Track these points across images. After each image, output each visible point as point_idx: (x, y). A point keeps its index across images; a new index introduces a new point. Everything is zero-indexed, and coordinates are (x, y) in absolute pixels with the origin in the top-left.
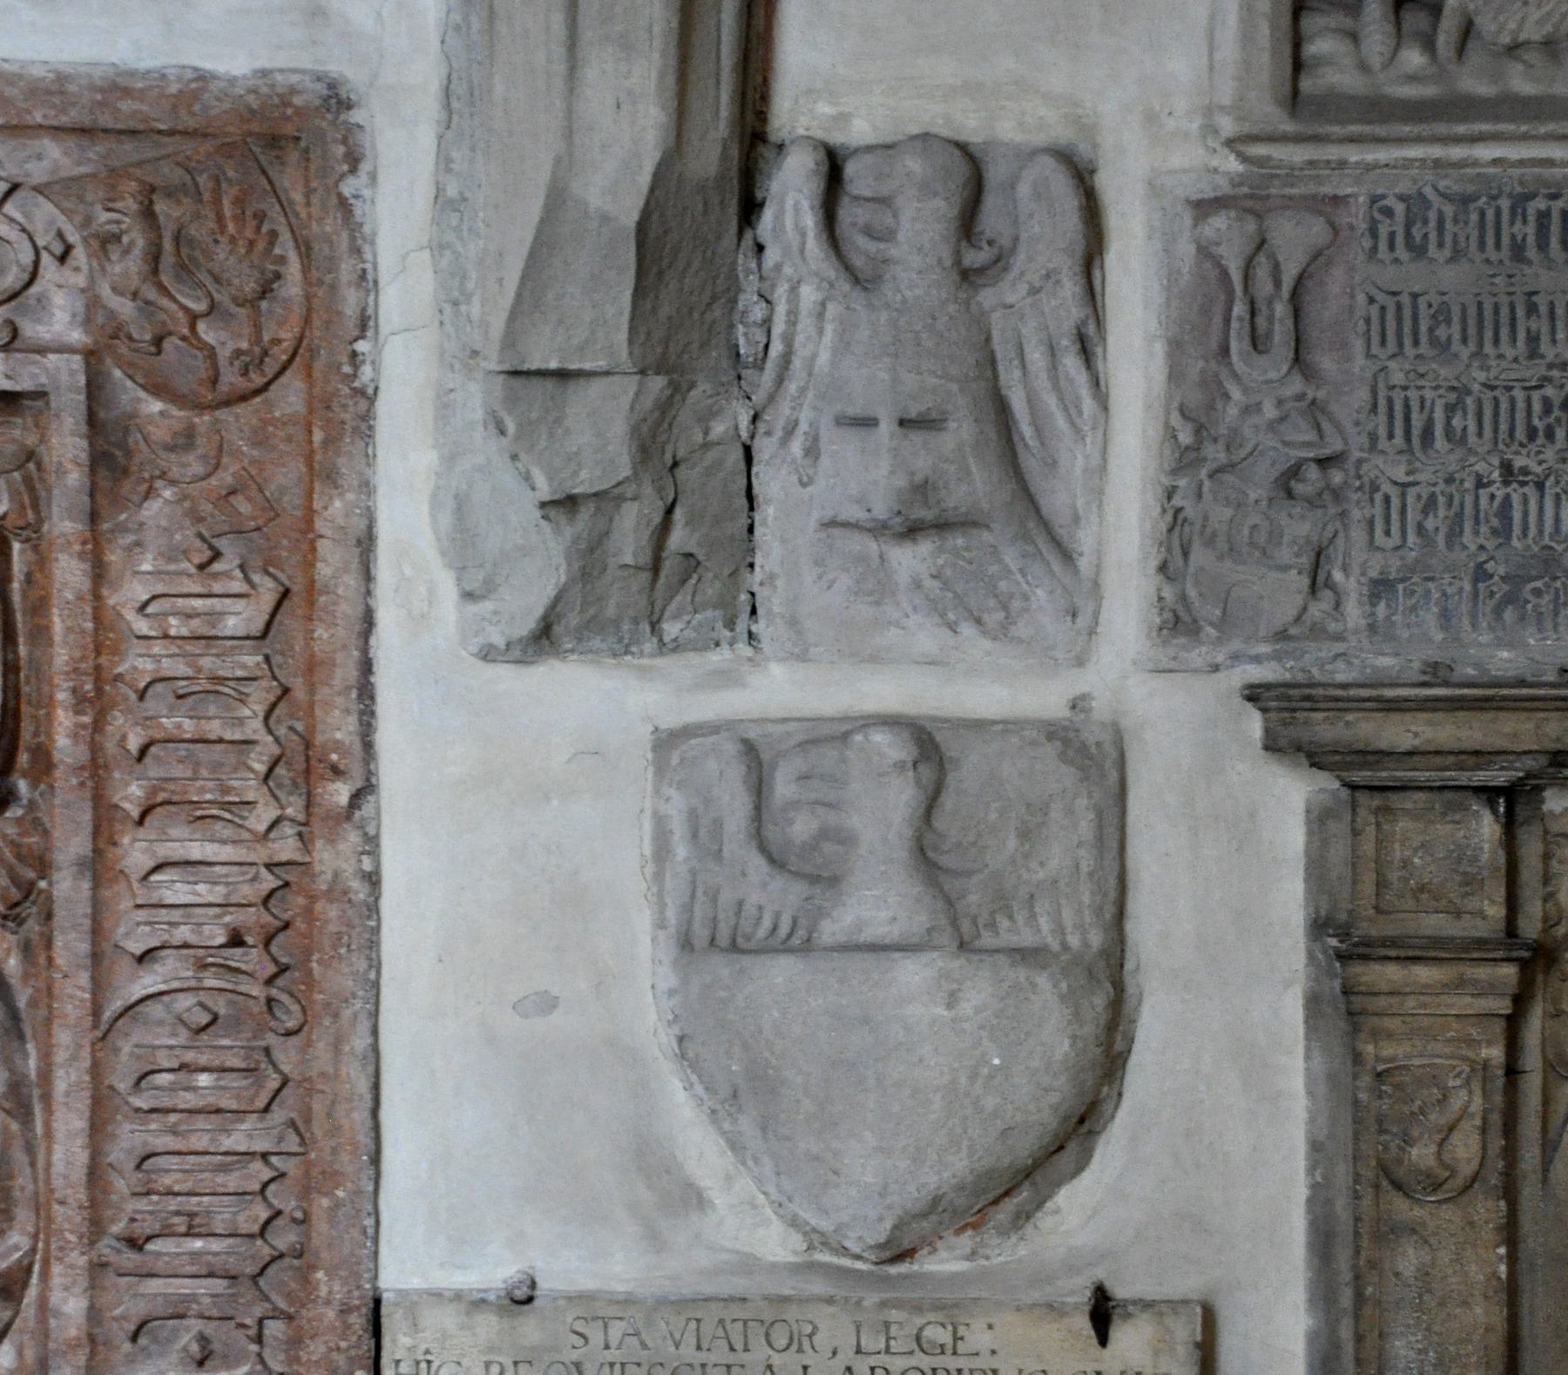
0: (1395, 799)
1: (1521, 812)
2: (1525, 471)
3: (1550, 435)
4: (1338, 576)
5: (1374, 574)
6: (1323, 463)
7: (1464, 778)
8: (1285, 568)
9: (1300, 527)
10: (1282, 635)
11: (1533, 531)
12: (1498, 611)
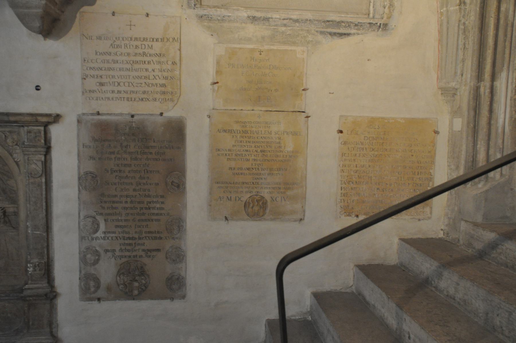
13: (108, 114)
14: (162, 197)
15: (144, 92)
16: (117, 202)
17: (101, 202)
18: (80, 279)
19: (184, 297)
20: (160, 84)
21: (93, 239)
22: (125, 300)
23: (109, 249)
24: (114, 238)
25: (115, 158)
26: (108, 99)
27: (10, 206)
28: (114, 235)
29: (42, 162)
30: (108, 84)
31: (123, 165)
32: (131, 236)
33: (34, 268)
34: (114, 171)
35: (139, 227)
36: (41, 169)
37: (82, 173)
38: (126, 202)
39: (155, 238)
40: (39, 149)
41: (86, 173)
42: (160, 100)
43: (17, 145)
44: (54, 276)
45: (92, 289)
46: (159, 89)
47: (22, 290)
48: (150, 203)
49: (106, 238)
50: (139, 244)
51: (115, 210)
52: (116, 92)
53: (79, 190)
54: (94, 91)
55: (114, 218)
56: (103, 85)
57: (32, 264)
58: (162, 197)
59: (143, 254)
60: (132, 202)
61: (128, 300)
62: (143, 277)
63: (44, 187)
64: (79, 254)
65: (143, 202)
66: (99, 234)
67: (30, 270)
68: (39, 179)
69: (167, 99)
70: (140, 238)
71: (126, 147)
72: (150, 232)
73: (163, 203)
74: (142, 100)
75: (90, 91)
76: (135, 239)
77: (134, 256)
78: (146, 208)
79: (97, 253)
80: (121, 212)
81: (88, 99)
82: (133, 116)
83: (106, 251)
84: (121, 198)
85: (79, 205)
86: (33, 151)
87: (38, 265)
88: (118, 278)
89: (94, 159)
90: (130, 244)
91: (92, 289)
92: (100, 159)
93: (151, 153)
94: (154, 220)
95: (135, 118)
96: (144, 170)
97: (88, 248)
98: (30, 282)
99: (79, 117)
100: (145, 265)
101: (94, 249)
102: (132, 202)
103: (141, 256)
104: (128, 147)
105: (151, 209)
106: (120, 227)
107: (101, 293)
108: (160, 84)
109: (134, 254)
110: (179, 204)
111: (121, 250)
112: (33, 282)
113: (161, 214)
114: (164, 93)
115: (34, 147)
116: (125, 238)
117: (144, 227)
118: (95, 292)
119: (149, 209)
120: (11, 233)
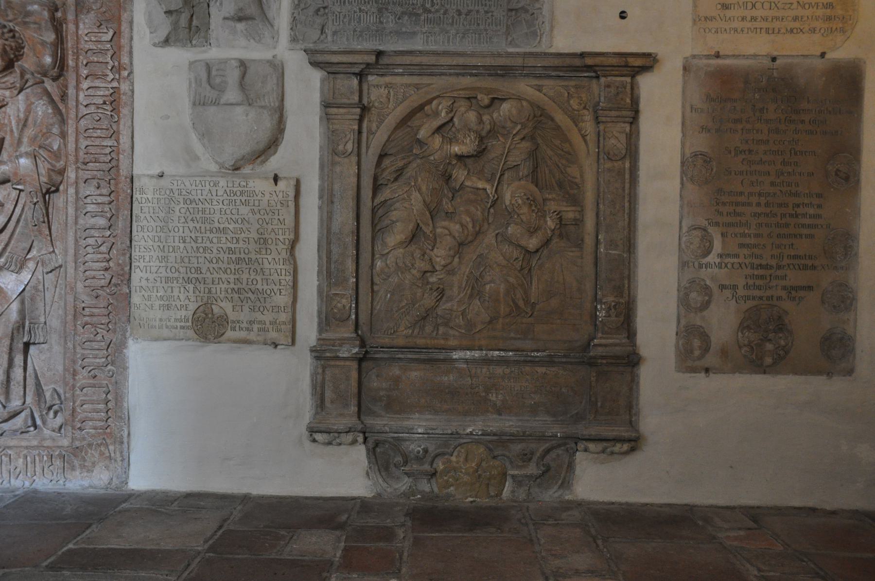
0: (337, 76)
1: (363, 80)
2: (364, 10)
3: (369, 3)
4: (327, 31)
5: (333, 30)
6: (325, 8)
7: (349, 70)
8: (315, 29)
9: (319, 20)
10: (315, 42)
11: (365, 22)
12: (358, 38)
13: (734, 56)
14: (819, 196)
15: (795, 19)
16: (744, 204)
17: (718, 204)
18: (677, 334)
19: (850, 372)
20: (823, 3)
21: (700, 266)
22: (751, 373)
23: (728, 283)
24: (737, 266)
25: (742, 129)
26: (736, 30)
27: (569, 209)
28: (735, 260)
29: (627, 134)
30: (736, 6)
31: (755, 142)
32: (764, 263)
33: (607, 312)
34: (741, 152)
35: (779, 247)
36: (625, 145)
37: (688, 152)
38: (759, 204)
39: (805, 267)
40: (624, 113)
41: (695, 155)
42: (822, 31)
43: (585, 108)
44: (636, 328)
45: (697, 353)
46: (820, 12)
47: (587, 347)
48: (798, 206)
49: (723, 265)
50: (777, 277)
51: (739, 218)
52: (749, 19)
53: (682, 183)
54: (712, 19)
55: (738, 230)
56: (727, 8)
57: (604, 304)
58: (819, 196)
59: (784, 294)
60: (767, 205)
61: (756, 374)
62: (781, 335)
63: (627, 176)
64: (678, 290)
65: (786, 205)
66: (712, 258)
67: (601, 314)
68: (620, 162)
69: (834, 29)
70: (779, 267)
71: (761, 110)
72: (795, 257)
73: (819, 206)
74: (792, 31)
75: (706, 18)
76: (771, 267)
77: (768, 298)
78: (791, 215)
79: (706, 290)
80: (749, 222)
81: (702, 30)
82: (774, 59)
83: (722, 287)
84: (751, 198)
85: (682, 207)
86: (614, 117)
87: (615, 306)
88: (740, 334)
89: (709, 131)
90: (762, 277)
91: (697, 353)
92: (717, 131)
93: (803, 122)
94: (804, 236)
95: (778, 62)
96: (791, 151)
97: (692, 282)
98: (600, 335)
99: (687, 61)
100: (786, 312)
101: (702, 283)
102: (767, 205)
103: (779, 298)
104: (765, 111)
105: (800, 217)
106: (747, 246)
107: (711, 360)
108: (823, 3)
109: (769, 293)
110: (847, 210)
111: (747, 287)
112: (604, 336)
113: (816, 226)
114: (829, 19)
115: (619, 109)
116: (755, 266)
117: (787, 247)
118: (702, 357)
119: (797, 216)
120: (571, 254)
